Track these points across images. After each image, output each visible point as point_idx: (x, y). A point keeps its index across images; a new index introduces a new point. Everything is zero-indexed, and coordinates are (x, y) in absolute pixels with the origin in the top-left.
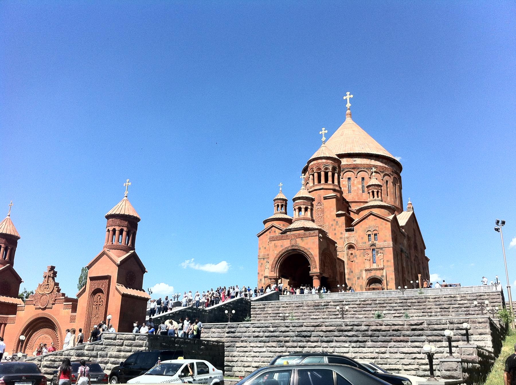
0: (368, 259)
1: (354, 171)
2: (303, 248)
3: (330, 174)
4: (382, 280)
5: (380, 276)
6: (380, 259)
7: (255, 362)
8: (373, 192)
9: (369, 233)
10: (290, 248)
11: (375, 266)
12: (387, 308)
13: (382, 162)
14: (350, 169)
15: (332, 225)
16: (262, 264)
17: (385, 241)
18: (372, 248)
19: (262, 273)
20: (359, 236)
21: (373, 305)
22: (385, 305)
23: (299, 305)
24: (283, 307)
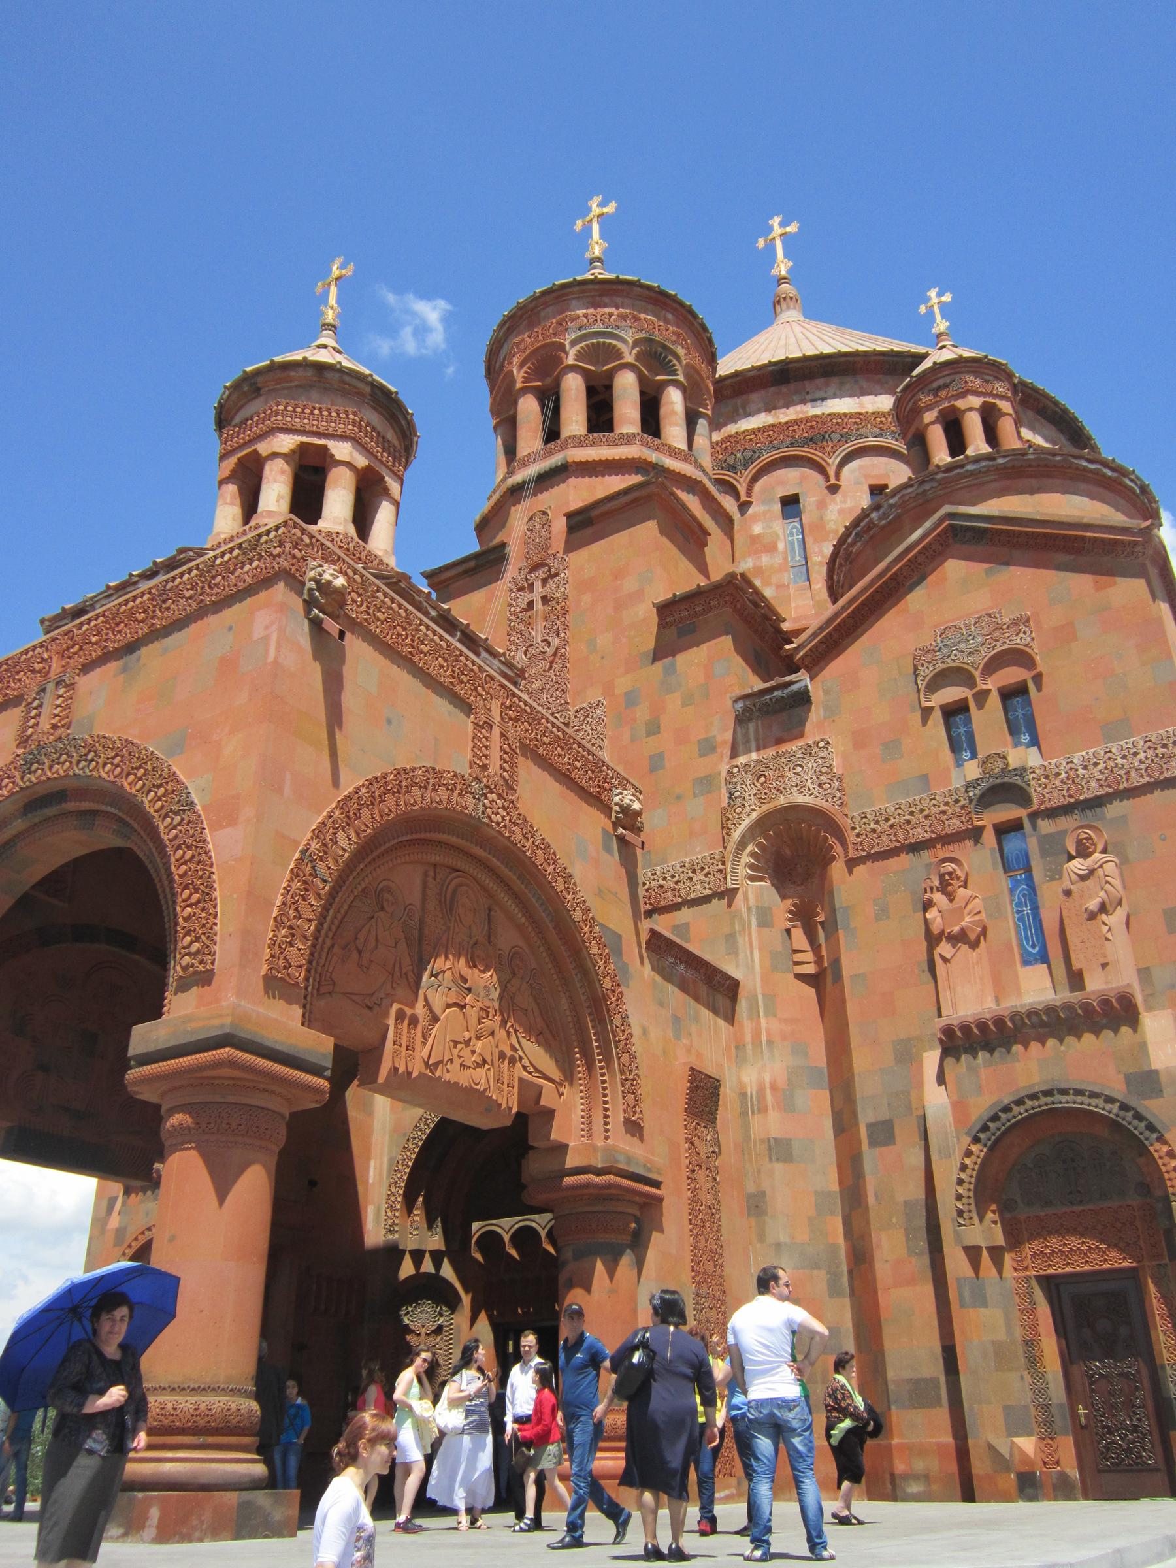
1: (817, 455)
3: (627, 386)
4: (1151, 1128)
5: (1117, 1087)
6: (1093, 905)
9: (952, 694)
17: (1113, 730)
18: (989, 818)
20: (859, 741)
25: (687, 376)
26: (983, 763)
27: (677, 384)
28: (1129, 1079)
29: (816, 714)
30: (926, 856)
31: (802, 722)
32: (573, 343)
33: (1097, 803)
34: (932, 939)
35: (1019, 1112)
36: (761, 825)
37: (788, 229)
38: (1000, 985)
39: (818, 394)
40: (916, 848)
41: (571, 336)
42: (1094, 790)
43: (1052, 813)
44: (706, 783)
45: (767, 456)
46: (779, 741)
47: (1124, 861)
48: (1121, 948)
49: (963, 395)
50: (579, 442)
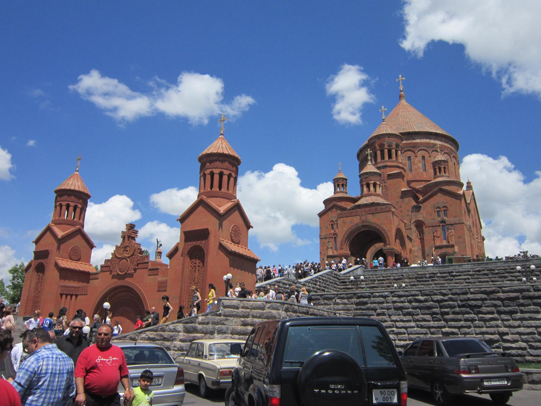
0: (438, 235)
1: (414, 150)
2: (375, 223)
3: (393, 151)
7: (400, 340)
9: (438, 210)
10: (360, 225)
11: (445, 243)
12: (509, 278)
14: (410, 147)
15: (398, 202)
16: (324, 243)
17: (455, 217)
18: (441, 224)
19: (325, 252)
21: (490, 276)
22: (506, 275)
23: (398, 277)
24: (379, 280)
26: (441, 218)
27: (400, 150)
28: (453, 252)
29: (422, 209)
30: (434, 228)
31: (420, 210)
32: (386, 144)
33: (452, 225)
34: (434, 237)
35: (442, 254)
36: (415, 221)
37: (403, 79)
38: (441, 242)
39: (414, 138)
40: (433, 226)
41: (386, 143)
42: (453, 223)
43: (448, 225)
44: (408, 215)
45: (406, 149)
46: (417, 212)
47: (455, 231)
48: (453, 240)
49: (442, 165)
50: (388, 161)
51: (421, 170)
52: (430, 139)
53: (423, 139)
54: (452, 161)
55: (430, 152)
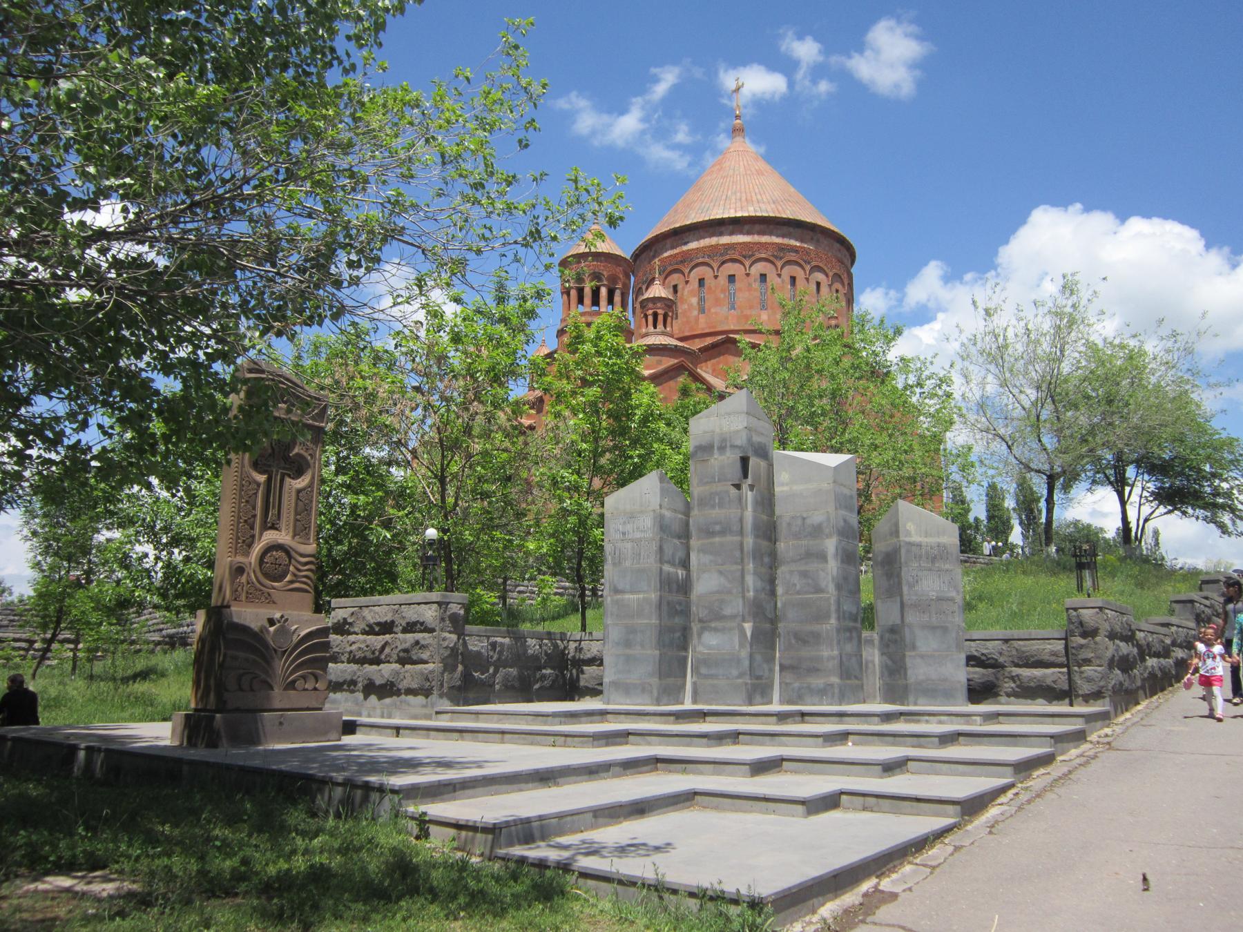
8: (655, 315)
13: (748, 233)
25: (608, 279)
27: (604, 285)
45: (670, 268)
51: (695, 313)
52: (721, 234)
53: (704, 238)
54: (779, 275)
55: (715, 266)
